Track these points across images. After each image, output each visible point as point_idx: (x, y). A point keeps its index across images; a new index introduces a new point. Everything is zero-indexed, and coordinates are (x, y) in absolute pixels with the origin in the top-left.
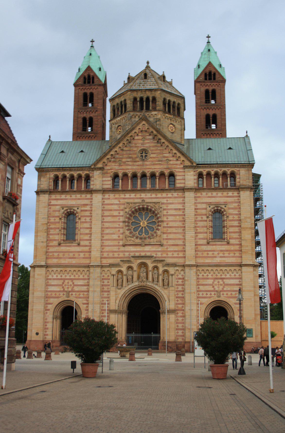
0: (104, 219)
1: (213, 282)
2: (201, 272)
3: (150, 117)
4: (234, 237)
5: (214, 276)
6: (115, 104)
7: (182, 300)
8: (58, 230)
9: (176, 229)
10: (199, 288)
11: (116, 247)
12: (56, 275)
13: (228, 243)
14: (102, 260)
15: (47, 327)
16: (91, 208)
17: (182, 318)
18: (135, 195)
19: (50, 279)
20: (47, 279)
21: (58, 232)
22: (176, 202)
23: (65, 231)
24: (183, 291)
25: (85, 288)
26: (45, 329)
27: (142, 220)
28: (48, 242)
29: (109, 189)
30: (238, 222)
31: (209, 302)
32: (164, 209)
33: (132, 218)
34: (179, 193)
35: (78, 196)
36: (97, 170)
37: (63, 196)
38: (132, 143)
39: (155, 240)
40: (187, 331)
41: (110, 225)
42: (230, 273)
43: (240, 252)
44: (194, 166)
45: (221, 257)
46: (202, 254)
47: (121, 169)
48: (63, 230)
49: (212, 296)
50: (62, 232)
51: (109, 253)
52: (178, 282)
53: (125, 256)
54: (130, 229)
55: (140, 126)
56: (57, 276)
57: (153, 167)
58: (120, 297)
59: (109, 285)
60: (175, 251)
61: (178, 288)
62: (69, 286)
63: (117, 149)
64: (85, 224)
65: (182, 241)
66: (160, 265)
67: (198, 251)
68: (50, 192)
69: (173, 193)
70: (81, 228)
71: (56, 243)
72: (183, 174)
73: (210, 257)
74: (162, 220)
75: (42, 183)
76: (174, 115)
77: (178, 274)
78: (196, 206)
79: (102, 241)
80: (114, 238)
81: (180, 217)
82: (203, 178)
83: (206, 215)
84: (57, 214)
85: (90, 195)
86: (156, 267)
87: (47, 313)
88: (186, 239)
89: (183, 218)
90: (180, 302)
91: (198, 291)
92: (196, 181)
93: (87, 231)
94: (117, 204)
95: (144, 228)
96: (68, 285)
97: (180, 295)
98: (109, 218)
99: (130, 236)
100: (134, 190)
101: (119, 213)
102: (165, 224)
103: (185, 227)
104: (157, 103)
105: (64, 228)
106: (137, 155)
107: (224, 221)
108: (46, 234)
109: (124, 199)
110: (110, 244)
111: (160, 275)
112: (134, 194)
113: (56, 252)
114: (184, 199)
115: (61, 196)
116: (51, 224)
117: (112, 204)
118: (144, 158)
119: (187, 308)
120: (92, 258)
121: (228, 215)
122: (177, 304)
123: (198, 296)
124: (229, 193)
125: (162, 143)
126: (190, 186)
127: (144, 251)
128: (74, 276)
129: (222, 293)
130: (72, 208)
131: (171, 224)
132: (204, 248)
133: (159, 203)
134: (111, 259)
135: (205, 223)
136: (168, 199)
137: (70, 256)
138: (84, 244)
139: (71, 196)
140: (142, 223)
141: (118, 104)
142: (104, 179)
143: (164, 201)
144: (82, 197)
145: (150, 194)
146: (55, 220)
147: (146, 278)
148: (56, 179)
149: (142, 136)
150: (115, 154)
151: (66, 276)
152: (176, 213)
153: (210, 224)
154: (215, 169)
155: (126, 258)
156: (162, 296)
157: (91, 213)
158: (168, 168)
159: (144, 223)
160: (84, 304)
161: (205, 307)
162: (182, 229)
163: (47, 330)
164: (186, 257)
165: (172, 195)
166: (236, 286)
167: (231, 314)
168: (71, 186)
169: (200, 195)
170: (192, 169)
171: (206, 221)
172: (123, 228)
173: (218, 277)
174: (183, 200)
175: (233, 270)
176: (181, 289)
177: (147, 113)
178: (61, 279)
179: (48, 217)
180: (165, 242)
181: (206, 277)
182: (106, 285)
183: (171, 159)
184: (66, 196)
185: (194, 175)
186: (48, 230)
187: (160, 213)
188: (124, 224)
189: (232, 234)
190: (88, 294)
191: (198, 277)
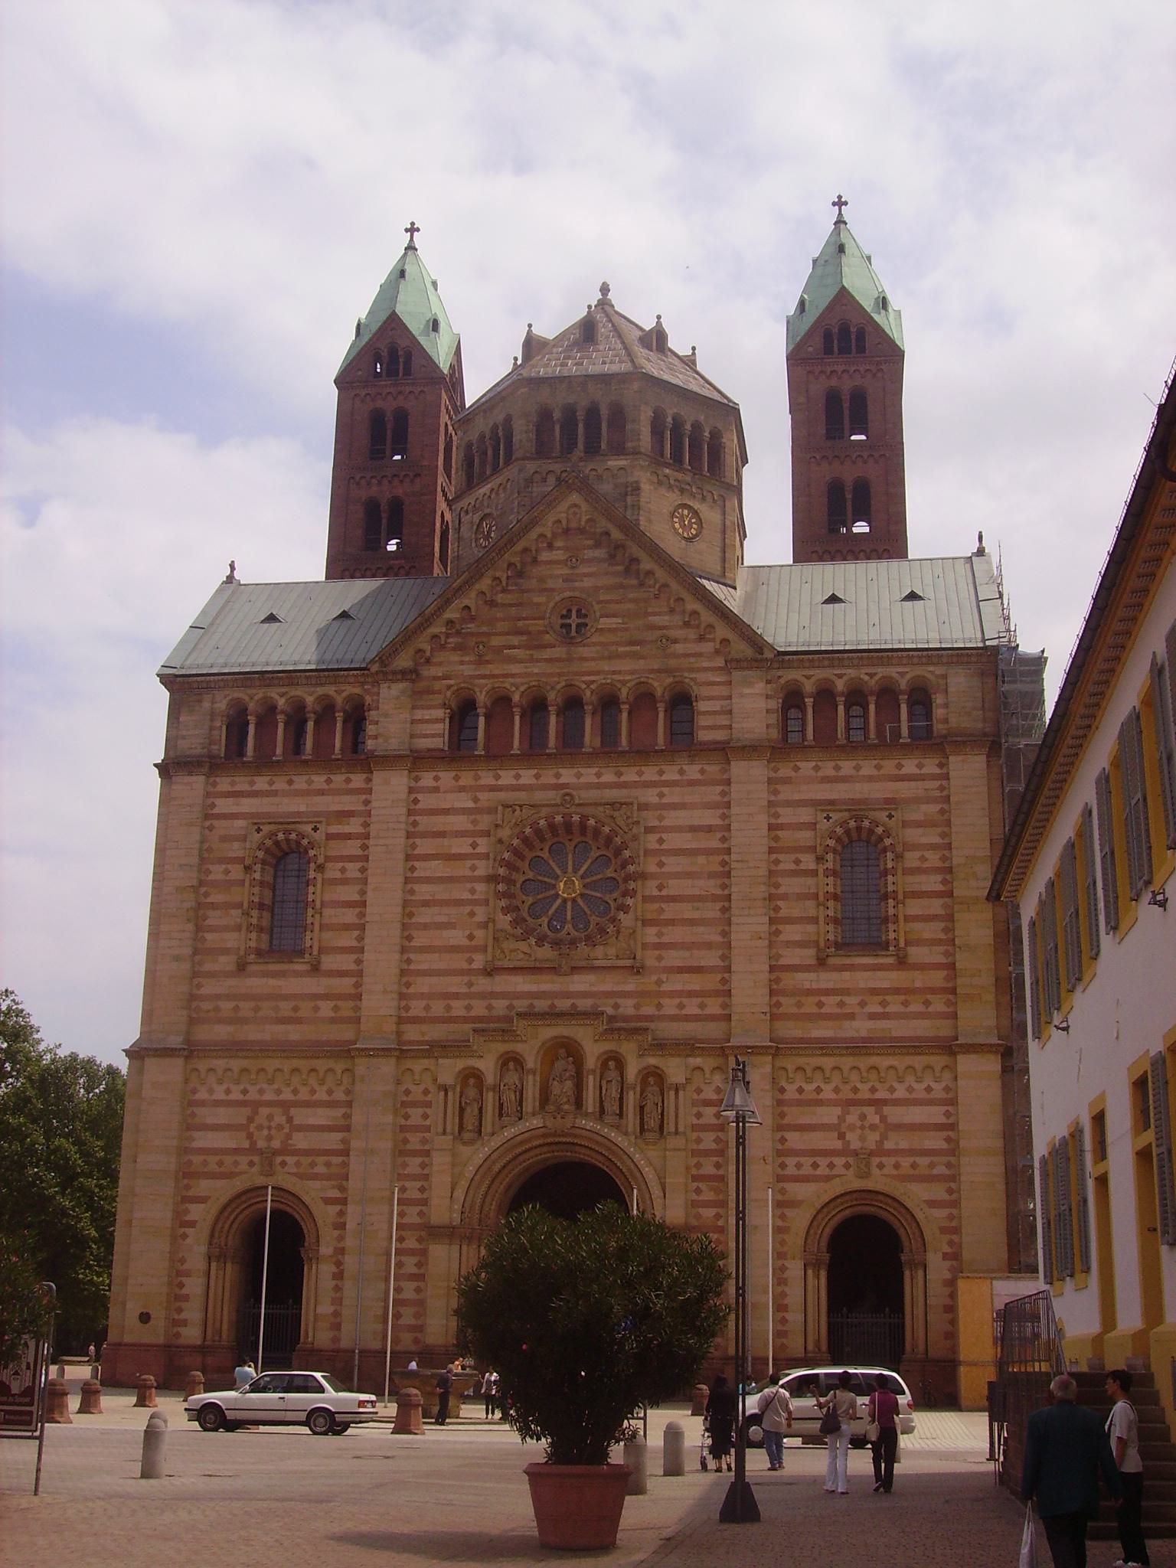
0: (413, 869)
2: (791, 1075)
3: (599, 477)
4: (926, 935)
5: (846, 1093)
6: (474, 436)
7: (717, 1191)
9: (695, 904)
10: (783, 1140)
11: (457, 979)
12: (224, 1087)
13: (902, 963)
14: (404, 1027)
15: (185, 1291)
16: (366, 825)
18: (537, 777)
19: (202, 1103)
20: (192, 1103)
23: (266, 915)
25: (333, 1140)
26: (179, 1298)
28: (198, 958)
30: (939, 878)
31: (826, 1198)
32: (649, 830)
33: (524, 865)
34: (706, 767)
35: (319, 780)
36: (392, 681)
37: (261, 783)
39: (612, 951)
42: (910, 1079)
44: (767, 660)
45: (873, 1016)
46: (799, 1005)
47: (484, 677)
48: (255, 913)
49: (835, 1172)
50: (254, 921)
52: (699, 1115)
53: (495, 1013)
54: (517, 909)
55: (561, 512)
56: (228, 1092)
58: (469, 1175)
59: (428, 1129)
60: (691, 994)
61: (699, 1141)
63: (470, 599)
64: (340, 889)
65: (720, 953)
66: (628, 1049)
67: (783, 993)
68: (210, 765)
71: (226, 962)
72: (724, 691)
73: (830, 1017)
75: (184, 733)
76: (696, 469)
77: (703, 1086)
78: (776, 815)
79: (405, 957)
81: (711, 858)
82: (802, 708)
83: (813, 849)
84: (236, 850)
85: (365, 776)
87: (185, 1236)
88: (733, 944)
89: (724, 863)
90: (708, 1195)
91: (779, 1153)
92: (773, 719)
93: (350, 916)
94: (464, 811)
95: (569, 904)
96: (269, 1128)
97: (709, 1168)
99: (513, 936)
100: (534, 752)
101: (474, 845)
102: (651, 888)
103: (728, 898)
104: (629, 427)
105: (261, 906)
106: (546, 622)
107: (885, 873)
108: (190, 927)
109: (493, 789)
110: (435, 966)
111: (628, 1088)
113: (229, 997)
114: (726, 788)
115: (252, 783)
117: (446, 812)
118: (573, 633)
121: (899, 849)
122: (695, 1204)
123: (779, 1171)
124: (903, 762)
125: (642, 576)
127: (568, 995)
128: (295, 1092)
129: (875, 1161)
131: (674, 887)
132: (807, 980)
136: (665, 790)
138: (334, 967)
139: (290, 782)
140: (562, 885)
141: (482, 437)
142: (419, 714)
143: (650, 796)
144: (332, 786)
145: (594, 771)
146: (227, 872)
147: (572, 1099)
149: (566, 549)
150: (463, 620)
151: (261, 1092)
152: (694, 845)
153: (831, 885)
155: (499, 1019)
157: (365, 847)
158: (667, 671)
159: (568, 887)
160: (328, 1201)
161: (809, 1216)
162: (719, 905)
163: (184, 1305)
165: (681, 772)
166: (932, 1133)
169: (793, 774)
171: (814, 873)
172: (486, 902)
173: (859, 1096)
174: (724, 794)
175: (919, 1067)
176: (714, 1146)
177: (591, 466)
178: (243, 1104)
179: (202, 860)
180: (650, 962)
181: (814, 1096)
182: (417, 1129)
184: (271, 783)
185: (768, 697)
186: (201, 912)
188: (492, 887)
189: (917, 926)
190: (345, 1165)
191: (780, 1097)
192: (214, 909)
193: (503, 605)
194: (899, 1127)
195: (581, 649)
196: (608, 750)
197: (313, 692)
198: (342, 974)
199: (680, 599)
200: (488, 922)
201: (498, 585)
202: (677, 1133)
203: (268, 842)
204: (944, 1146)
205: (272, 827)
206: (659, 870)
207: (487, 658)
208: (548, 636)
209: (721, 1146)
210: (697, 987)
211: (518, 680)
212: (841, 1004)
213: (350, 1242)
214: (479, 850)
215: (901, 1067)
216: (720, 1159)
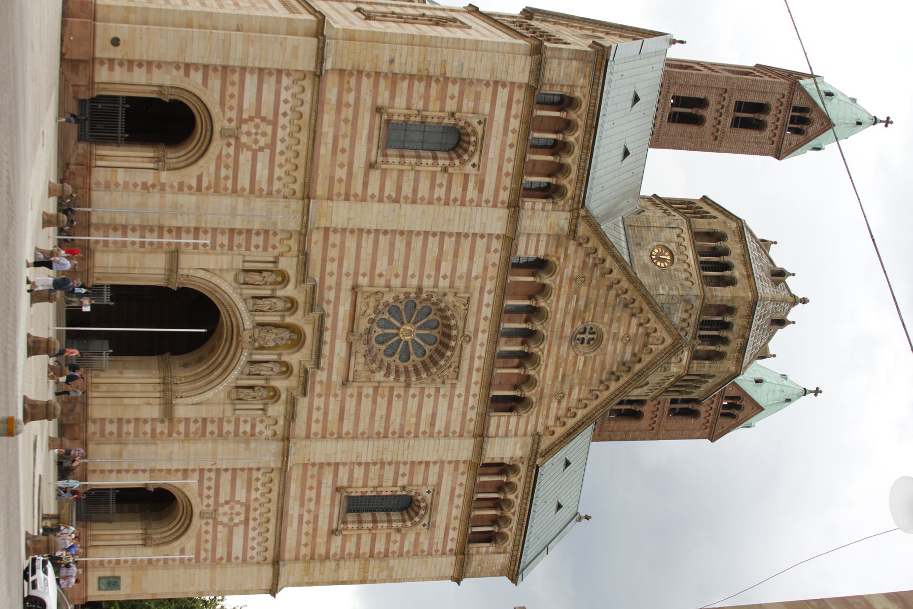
1: (238, 502)
2: (268, 475)
4: (348, 544)
5: (253, 505)
7: (196, 432)
8: (420, 106)
11: (352, 266)
12: (290, 98)
13: (333, 532)
14: (322, 233)
17: (149, 431)
18: (485, 318)
19: (279, 81)
21: (414, 107)
22: (453, 417)
24: (220, 435)
25: (244, 181)
27: (418, 328)
29: (513, 252)
30: (382, 550)
31: (188, 494)
32: (438, 390)
34: (473, 422)
35: (509, 167)
36: (571, 222)
37: (515, 124)
38: (623, 311)
39: (360, 367)
40: (116, 448)
41: (415, 254)
42: (260, 539)
43: (308, 558)
44: (535, 460)
45: (301, 517)
47: (561, 282)
48: (418, 119)
49: (205, 500)
51: (338, 248)
53: (326, 291)
55: (662, 333)
56: (286, 102)
57: (550, 361)
59: (248, 249)
60: (326, 414)
61: (229, 422)
62: (253, 137)
63: (616, 274)
64: (428, 183)
65: (351, 431)
66: (293, 382)
69: (475, 410)
70: (418, 172)
71: (384, 98)
72: (521, 431)
74: (413, 385)
75: (563, 65)
77: (265, 424)
80: (379, 263)
83: (410, 483)
84: (468, 105)
85: (507, 201)
86: (287, 370)
93: (407, 190)
94: (470, 270)
95: (395, 331)
96: (256, 134)
98: (436, 250)
103: (386, 437)
108: (414, 71)
109: (482, 289)
110: (363, 251)
112: (489, 316)
113: (357, 99)
115: (516, 117)
116: (440, 84)
117: (471, 258)
119: (175, 447)
120: (330, 202)
124: (457, 531)
126: (489, 447)
128: (282, 153)
129: (211, 521)
130: (479, 149)
131: (397, 405)
132: (328, 481)
133: (457, 378)
134: (320, 253)
135: (390, 483)
136: (462, 398)
137: (340, 138)
139: (511, 146)
140: (409, 328)
142: (543, 239)
143: (460, 389)
144: (503, 177)
145: (483, 355)
146: (452, 97)
148: (565, 102)
149: (636, 335)
151: (284, 127)
154: (519, 501)
155: (321, 294)
156: (209, 387)
158: (541, 398)
159: (408, 332)
160: (200, 178)
162: (382, 431)
164: (307, 442)
165: (473, 408)
167: (155, 536)
168: (539, 147)
169: (460, 471)
170: (528, 453)
175: (267, 544)
176: (225, 430)
180: (349, 391)
181: (253, 487)
183: (564, 404)
184: (513, 131)
185: (512, 458)
187: (430, 380)
192: (426, 87)
193: (607, 295)
194: (231, 533)
195: (566, 344)
196: (497, 358)
197: (574, 164)
198: (365, 185)
199: (586, 406)
200: (389, 287)
201: (622, 290)
202: (235, 410)
203: (469, 130)
204: (218, 556)
205: (480, 135)
206: (410, 395)
207: (574, 285)
208: (580, 323)
209: (224, 435)
210: (330, 418)
211: (554, 304)
212: (310, 500)
213: (169, 198)
214: (441, 280)
215: (268, 535)
216: (216, 434)
